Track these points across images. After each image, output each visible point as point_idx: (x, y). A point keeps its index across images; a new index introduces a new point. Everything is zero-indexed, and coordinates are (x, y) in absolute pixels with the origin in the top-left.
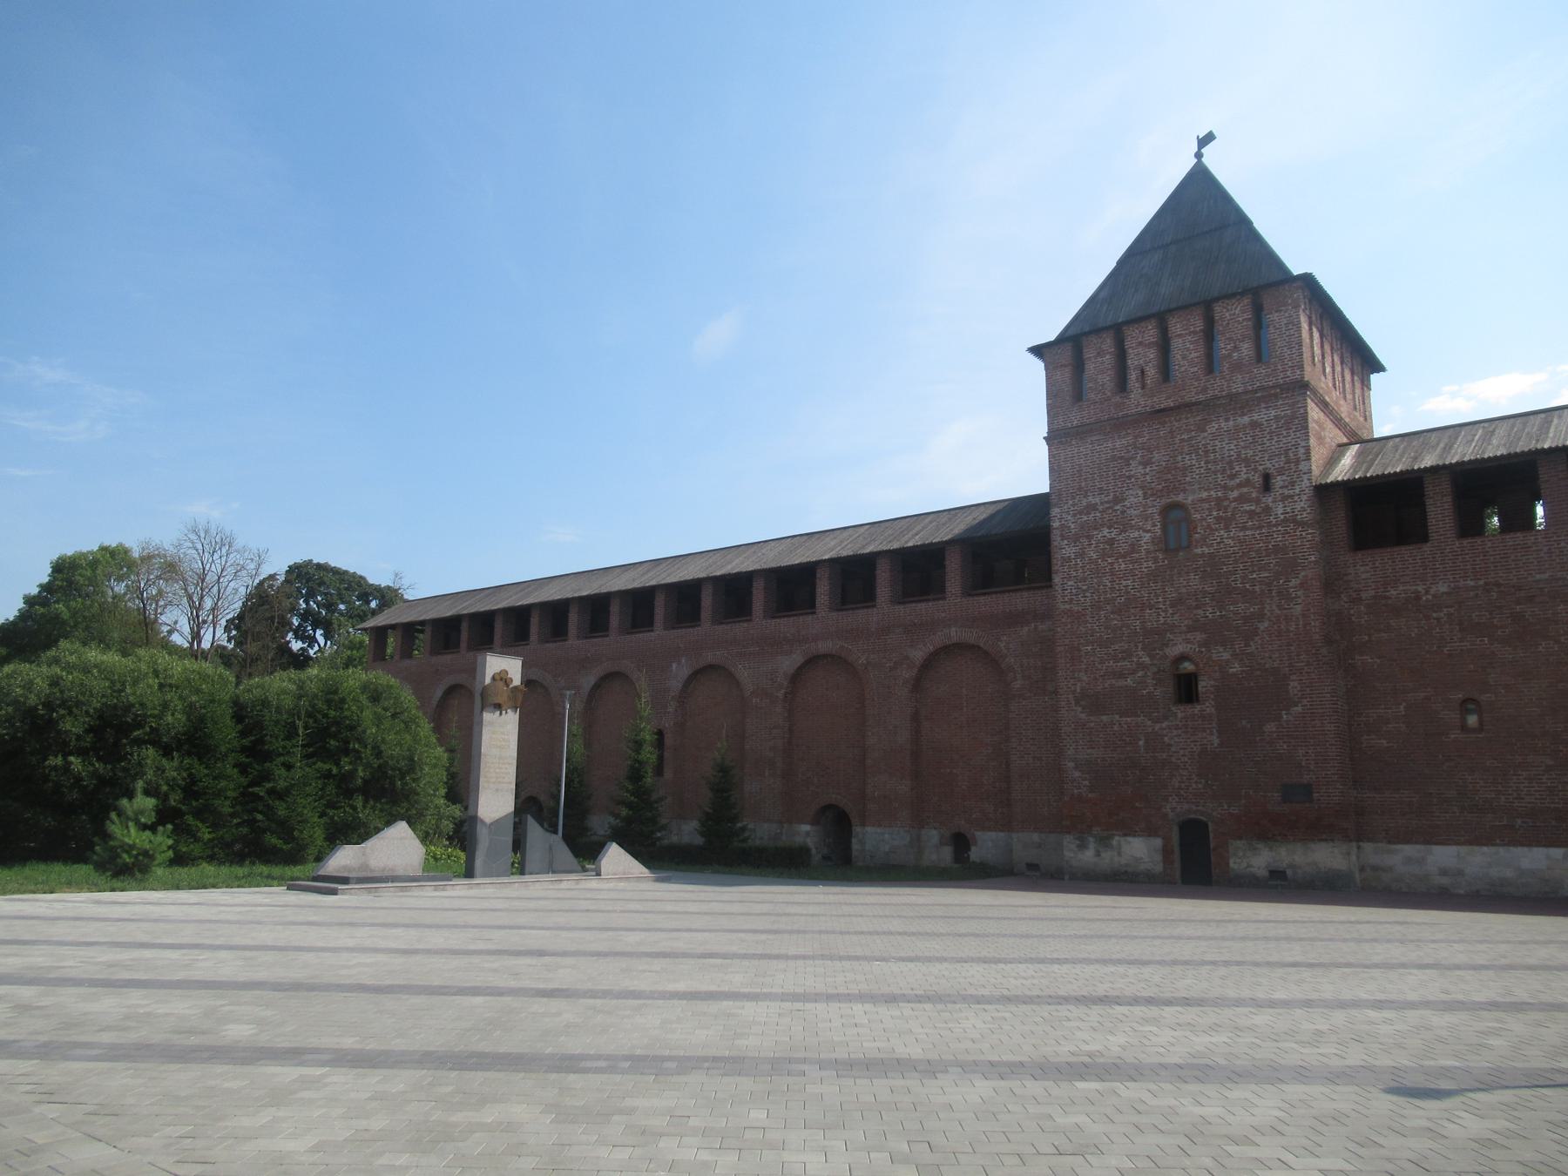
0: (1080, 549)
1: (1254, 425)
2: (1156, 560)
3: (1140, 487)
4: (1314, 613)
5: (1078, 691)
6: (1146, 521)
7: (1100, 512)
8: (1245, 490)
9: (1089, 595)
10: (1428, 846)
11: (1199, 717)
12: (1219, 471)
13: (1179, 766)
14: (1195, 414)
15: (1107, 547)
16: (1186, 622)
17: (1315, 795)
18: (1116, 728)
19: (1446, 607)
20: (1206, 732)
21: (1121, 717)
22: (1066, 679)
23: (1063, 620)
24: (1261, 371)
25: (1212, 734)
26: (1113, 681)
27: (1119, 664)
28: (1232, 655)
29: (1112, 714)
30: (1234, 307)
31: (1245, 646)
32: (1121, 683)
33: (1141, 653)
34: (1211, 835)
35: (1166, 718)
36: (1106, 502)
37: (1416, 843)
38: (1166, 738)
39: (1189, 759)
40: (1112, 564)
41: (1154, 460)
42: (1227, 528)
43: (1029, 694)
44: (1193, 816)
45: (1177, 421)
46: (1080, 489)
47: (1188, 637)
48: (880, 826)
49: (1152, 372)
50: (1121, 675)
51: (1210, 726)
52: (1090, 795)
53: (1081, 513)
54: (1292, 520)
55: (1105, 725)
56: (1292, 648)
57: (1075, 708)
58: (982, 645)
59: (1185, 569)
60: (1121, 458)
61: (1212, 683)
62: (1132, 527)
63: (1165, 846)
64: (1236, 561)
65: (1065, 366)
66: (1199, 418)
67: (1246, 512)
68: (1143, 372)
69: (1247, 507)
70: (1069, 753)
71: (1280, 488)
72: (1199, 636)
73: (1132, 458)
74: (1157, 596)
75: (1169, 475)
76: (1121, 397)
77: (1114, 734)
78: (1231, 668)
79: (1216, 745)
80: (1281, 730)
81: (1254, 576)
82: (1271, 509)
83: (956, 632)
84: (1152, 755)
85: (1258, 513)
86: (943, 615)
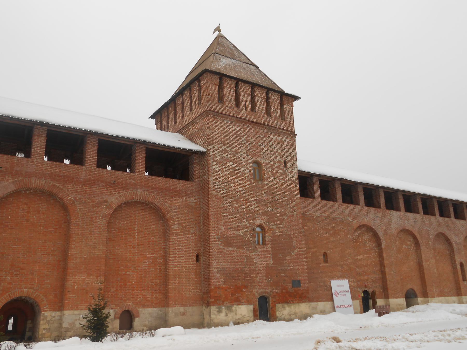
0: (221, 168)
1: (282, 142)
2: (251, 183)
3: (245, 150)
4: (299, 216)
5: (220, 234)
6: (248, 165)
7: (230, 154)
8: (279, 164)
9: (225, 190)
10: (317, 303)
12: (272, 154)
13: (259, 272)
14: (264, 129)
15: (232, 170)
16: (262, 211)
17: (301, 285)
18: (235, 254)
20: (267, 258)
21: (237, 249)
22: (214, 228)
23: (213, 199)
24: (283, 123)
25: (270, 259)
27: (237, 224)
28: (276, 227)
29: (234, 247)
30: (276, 96)
31: (281, 225)
32: (237, 233)
33: (246, 221)
34: (271, 302)
35: (254, 251)
36: (233, 151)
37: (315, 302)
38: (254, 260)
39: (263, 269)
41: (250, 141)
42: (274, 176)
43: (181, 233)
44: (264, 294)
45: (258, 129)
46: (221, 141)
47: (263, 217)
48: (77, 309)
49: (249, 106)
50: (237, 229)
52: (224, 286)
55: (230, 252)
56: (294, 228)
57: (217, 242)
58: (156, 203)
59: (261, 189)
60: (238, 135)
61: (270, 237)
62: (242, 165)
63: (254, 309)
64: (277, 191)
65: (215, 84)
66: (265, 131)
68: (245, 103)
69: (280, 171)
70: (215, 264)
71: (290, 168)
72: (266, 218)
73: (242, 136)
74: (251, 197)
75: (256, 149)
76: (238, 110)
77: (234, 257)
78: (276, 232)
81: (283, 198)
82: (287, 174)
83: (141, 193)
84: (249, 267)
85: (283, 175)
86: (133, 182)
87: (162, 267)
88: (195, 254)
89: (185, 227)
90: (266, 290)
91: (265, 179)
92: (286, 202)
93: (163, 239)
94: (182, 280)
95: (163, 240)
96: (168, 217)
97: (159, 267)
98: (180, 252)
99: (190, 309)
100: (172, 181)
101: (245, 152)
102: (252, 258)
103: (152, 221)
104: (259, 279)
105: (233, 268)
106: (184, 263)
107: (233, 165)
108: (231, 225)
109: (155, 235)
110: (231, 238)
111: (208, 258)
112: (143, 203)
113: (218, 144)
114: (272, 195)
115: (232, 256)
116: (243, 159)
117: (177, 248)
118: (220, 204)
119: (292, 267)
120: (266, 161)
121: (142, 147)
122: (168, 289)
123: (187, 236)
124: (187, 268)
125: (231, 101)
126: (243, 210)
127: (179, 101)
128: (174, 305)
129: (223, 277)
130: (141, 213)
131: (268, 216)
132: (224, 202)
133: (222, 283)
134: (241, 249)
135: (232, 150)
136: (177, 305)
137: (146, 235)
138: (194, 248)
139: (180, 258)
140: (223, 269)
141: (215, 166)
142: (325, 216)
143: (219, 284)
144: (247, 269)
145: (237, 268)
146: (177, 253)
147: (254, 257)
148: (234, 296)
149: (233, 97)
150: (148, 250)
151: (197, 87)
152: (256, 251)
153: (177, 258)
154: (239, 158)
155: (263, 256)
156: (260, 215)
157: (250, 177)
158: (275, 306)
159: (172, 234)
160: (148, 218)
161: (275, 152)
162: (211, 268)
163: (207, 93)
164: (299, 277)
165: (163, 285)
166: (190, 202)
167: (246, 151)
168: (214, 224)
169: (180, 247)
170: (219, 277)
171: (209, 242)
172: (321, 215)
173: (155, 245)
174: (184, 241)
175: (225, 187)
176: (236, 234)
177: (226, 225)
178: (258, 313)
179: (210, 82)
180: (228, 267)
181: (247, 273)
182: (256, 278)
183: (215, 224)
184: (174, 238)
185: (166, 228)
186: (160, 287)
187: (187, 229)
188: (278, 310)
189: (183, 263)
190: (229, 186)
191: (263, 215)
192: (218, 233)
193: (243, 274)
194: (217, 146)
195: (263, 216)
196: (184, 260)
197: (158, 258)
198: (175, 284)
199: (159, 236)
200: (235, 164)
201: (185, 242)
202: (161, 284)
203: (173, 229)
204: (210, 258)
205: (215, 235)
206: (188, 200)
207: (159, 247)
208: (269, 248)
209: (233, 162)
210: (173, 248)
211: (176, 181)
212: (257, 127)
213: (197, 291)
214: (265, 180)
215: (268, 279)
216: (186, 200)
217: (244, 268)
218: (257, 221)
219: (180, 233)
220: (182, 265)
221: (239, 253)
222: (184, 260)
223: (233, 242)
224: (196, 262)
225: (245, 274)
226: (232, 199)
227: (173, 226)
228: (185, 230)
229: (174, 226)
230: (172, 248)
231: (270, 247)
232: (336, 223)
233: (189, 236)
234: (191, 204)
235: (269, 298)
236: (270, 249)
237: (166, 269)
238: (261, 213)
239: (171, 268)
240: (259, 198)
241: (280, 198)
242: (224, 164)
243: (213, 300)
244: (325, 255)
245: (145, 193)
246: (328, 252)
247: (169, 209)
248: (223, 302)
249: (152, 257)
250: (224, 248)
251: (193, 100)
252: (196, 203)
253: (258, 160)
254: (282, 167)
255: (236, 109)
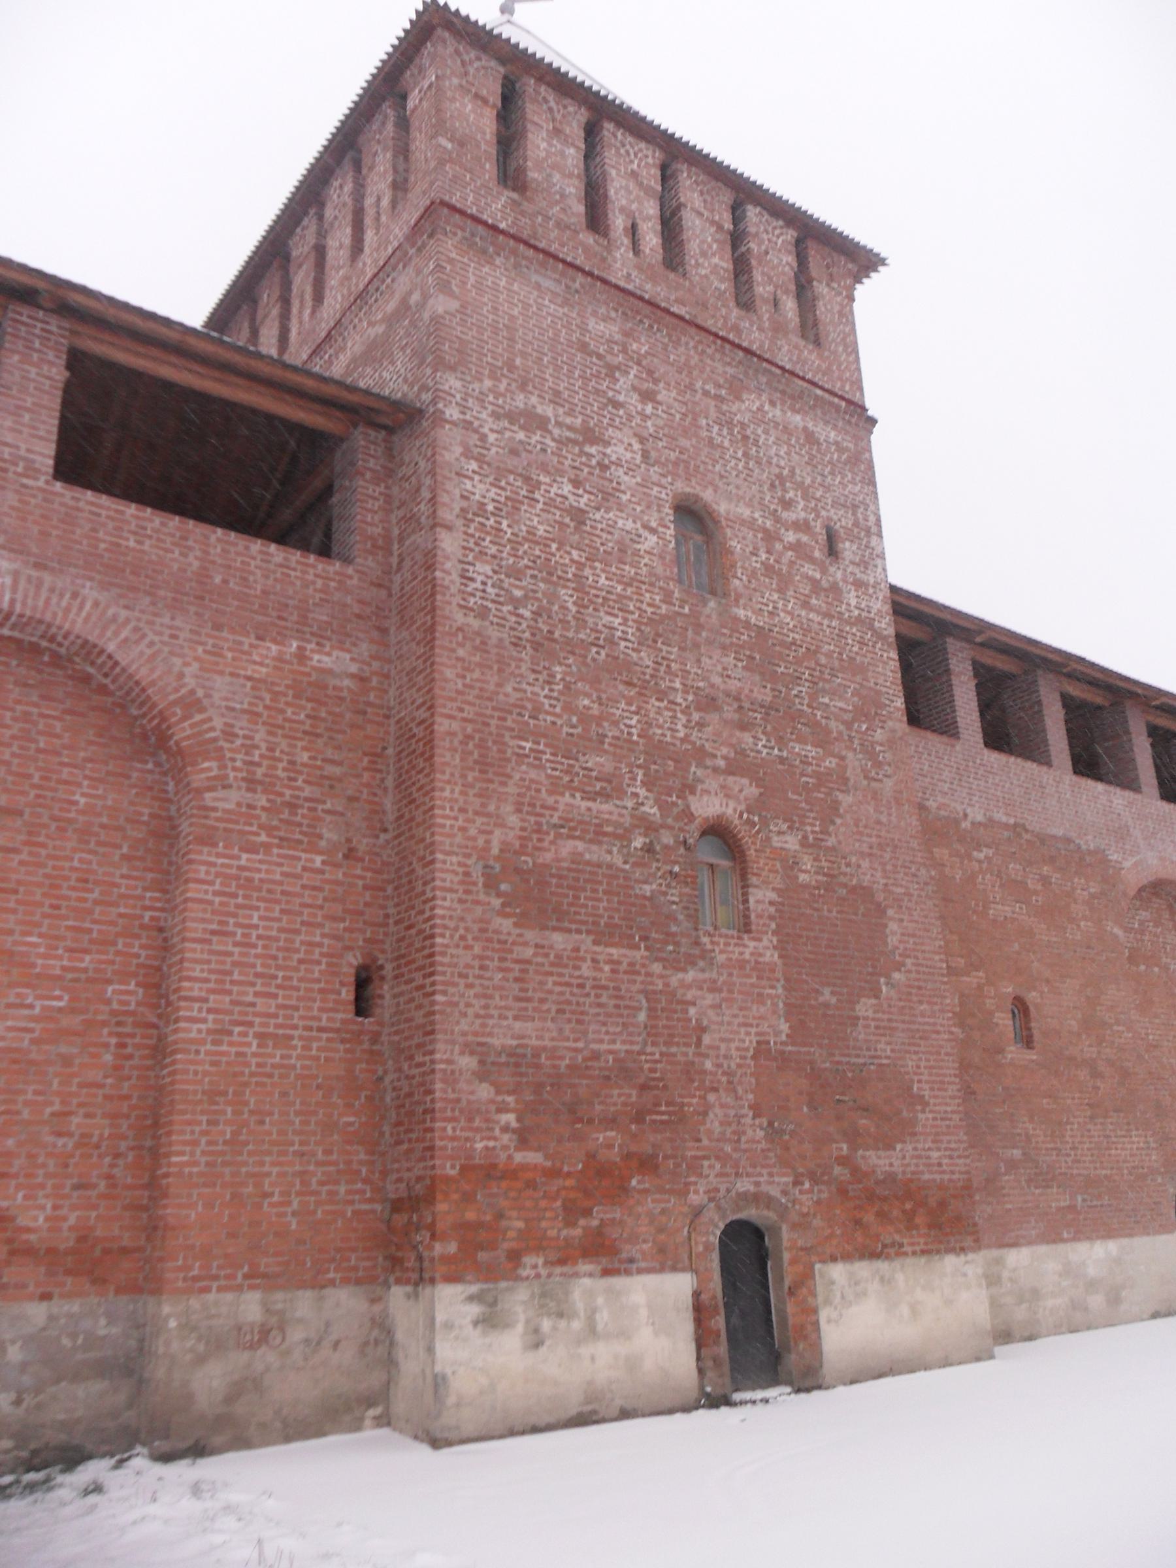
1: (811, 438)
2: (668, 598)
5: (495, 851)
8: (805, 538)
11: (752, 969)
15: (567, 520)
16: (725, 750)
18: (586, 970)
19: (987, 846)
20: (763, 1003)
21: (595, 943)
22: (463, 810)
23: (461, 652)
26: (580, 846)
29: (579, 932)
32: (594, 854)
33: (642, 792)
34: (786, 1256)
35: (691, 962)
36: (570, 428)
38: (692, 1011)
40: (580, 566)
42: (781, 591)
43: (263, 838)
46: (511, 367)
49: (651, 240)
50: (598, 833)
51: (773, 992)
52: (519, 1157)
53: (511, 417)
54: (864, 622)
57: (482, 897)
58: (111, 647)
60: (600, 357)
61: (773, 896)
63: (696, 1294)
65: (485, 101)
67: (807, 577)
69: (808, 569)
70: (464, 1025)
73: (618, 368)
79: (784, 1038)
80: (880, 1015)
84: (664, 1049)
87: (132, 1036)
88: (350, 965)
89: (293, 807)
90: (757, 1184)
91: (738, 597)
92: (844, 722)
93: (151, 870)
94: (262, 1122)
95: (150, 875)
96: (188, 738)
97: (119, 1035)
98: (255, 946)
99: (303, 1304)
100: (219, 540)
101: (637, 446)
102: (680, 1002)
103: (91, 760)
104: (721, 1124)
105: (576, 1050)
106: (276, 1016)
107: (571, 498)
108: (561, 807)
109: (99, 843)
110: (560, 877)
111: (422, 987)
112: (35, 649)
113: (493, 376)
114: (774, 677)
115: (568, 984)
116: (626, 478)
117: (237, 925)
118: (499, 685)
119: (888, 1057)
120: (739, 510)
121: (43, 330)
122: (166, 1175)
123: (299, 859)
124: (295, 1048)
125: (563, 196)
126: (629, 734)
127: (301, 246)
128: (195, 1279)
129: (512, 1105)
130: (18, 702)
131: (758, 781)
132: (521, 676)
133: (506, 1138)
134: (612, 945)
135: (568, 420)
136: (216, 1278)
137: (41, 839)
138: (345, 929)
139: (253, 984)
140: (510, 1055)
141: (472, 479)
142: (1006, 826)
143: (491, 1144)
144: (656, 1062)
145: (593, 1051)
146: (230, 954)
147: (689, 996)
148: (582, 1222)
149: (576, 182)
150: (44, 930)
151: (390, 127)
152: (701, 964)
153: (232, 982)
154: (603, 467)
155: (740, 992)
156: (716, 770)
157: (660, 570)
158: (808, 1275)
159: (208, 841)
160: (58, 736)
161: (779, 476)
162: (440, 1046)
163: (440, 127)
164: (923, 1111)
165: (133, 1148)
166: (323, 671)
167: (641, 443)
168: (462, 793)
169: (255, 921)
170: (492, 1101)
171: (433, 889)
172: (991, 820)
173: (96, 902)
174: (281, 883)
175: (526, 596)
176: (587, 856)
177: (532, 805)
178: (719, 1322)
179: (455, 81)
180: (544, 1048)
181: (657, 1087)
182: (705, 1114)
183: (471, 792)
184: (214, 865)
185: (173, 808)
186: (112, 1166)
187: (303, 816)
188: (828, 1302)
189: (269, 1015)
190: (553, 597)
191: (732, 774)
192: (488, 842)
193: (634, 1093)
194: (488, 383)
195: (731, 779)
196: (275, 996)
197: (109, 982)
198: (209, 1143)
199: (125, 850)
200: (580, 492)
201: (283, 893)
202: (123, 1146)
203: (215, 809)
204: (433, 984)
205: (468, 856)
206: (316, 657)
207: (121, 915)
208: (768, 953)
209: (570, 480)
210: (210, 921)
211: (247, 548)
212: (692, 344)
213: (349, 1192)
214: (737, 600)
215: (771, 1124)
216: (301, 656)
217: (639, 1053)
218: (705, 798)
219: (257, 834)
220: (263, 1025)
221: (607, 968)
222: (275, 996)
223: (571, 904)
224: (351, 1016)
225: (644, 1087)
226: (569, 666)
227: (210, 789)
228: (287, 822)
229: (221, 793)
230: (203, 920)
231: (775, 948)
232: (1052, 860)
233: (312, 861)
234: (333, 682)
235: (775, 1231)
236: (771, 956)
237: (160, 1051)
238: (722, 763)
239: (192, 1041)
240: (712, 686)
241: (813, 697)
242: (527, 479)
243: (452, 1248)
244: (1020, 1008)
245: (39, 584)
246: (1032, 997)
247: (192, 692)
248: (515, 1257)
249: (70, 976)
250: (518, 931)
251: (369, 201)
252: (361, 679)
253: (702, 494)
254: (817, 554)
255: (589, 239)
